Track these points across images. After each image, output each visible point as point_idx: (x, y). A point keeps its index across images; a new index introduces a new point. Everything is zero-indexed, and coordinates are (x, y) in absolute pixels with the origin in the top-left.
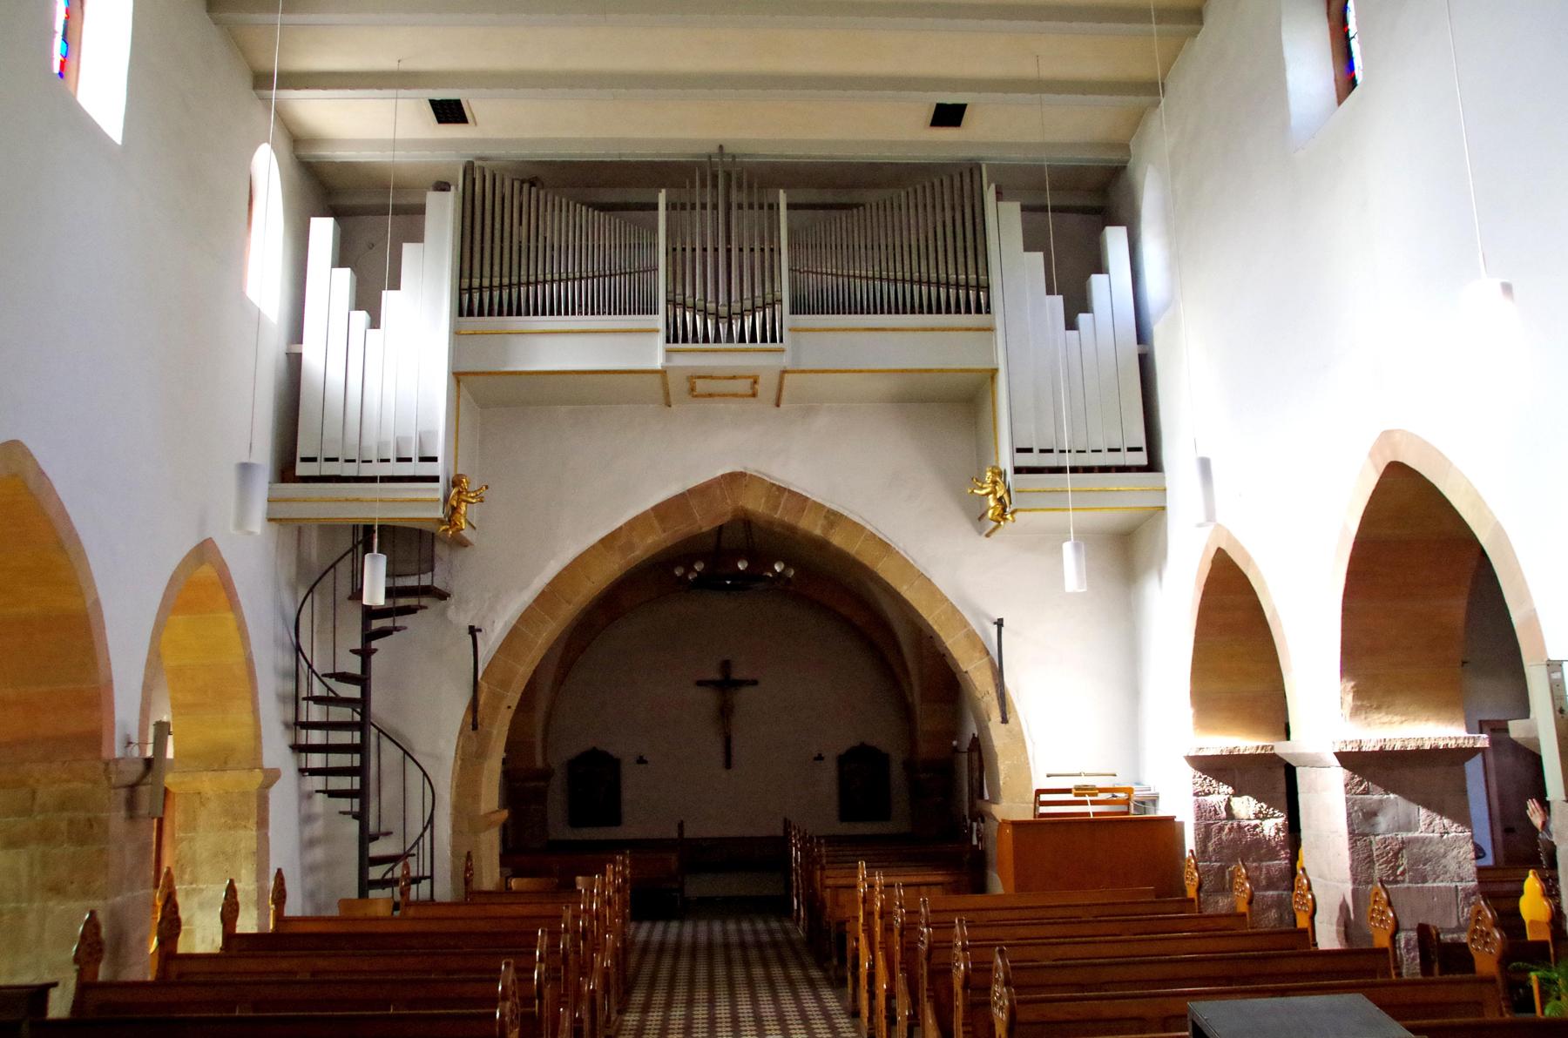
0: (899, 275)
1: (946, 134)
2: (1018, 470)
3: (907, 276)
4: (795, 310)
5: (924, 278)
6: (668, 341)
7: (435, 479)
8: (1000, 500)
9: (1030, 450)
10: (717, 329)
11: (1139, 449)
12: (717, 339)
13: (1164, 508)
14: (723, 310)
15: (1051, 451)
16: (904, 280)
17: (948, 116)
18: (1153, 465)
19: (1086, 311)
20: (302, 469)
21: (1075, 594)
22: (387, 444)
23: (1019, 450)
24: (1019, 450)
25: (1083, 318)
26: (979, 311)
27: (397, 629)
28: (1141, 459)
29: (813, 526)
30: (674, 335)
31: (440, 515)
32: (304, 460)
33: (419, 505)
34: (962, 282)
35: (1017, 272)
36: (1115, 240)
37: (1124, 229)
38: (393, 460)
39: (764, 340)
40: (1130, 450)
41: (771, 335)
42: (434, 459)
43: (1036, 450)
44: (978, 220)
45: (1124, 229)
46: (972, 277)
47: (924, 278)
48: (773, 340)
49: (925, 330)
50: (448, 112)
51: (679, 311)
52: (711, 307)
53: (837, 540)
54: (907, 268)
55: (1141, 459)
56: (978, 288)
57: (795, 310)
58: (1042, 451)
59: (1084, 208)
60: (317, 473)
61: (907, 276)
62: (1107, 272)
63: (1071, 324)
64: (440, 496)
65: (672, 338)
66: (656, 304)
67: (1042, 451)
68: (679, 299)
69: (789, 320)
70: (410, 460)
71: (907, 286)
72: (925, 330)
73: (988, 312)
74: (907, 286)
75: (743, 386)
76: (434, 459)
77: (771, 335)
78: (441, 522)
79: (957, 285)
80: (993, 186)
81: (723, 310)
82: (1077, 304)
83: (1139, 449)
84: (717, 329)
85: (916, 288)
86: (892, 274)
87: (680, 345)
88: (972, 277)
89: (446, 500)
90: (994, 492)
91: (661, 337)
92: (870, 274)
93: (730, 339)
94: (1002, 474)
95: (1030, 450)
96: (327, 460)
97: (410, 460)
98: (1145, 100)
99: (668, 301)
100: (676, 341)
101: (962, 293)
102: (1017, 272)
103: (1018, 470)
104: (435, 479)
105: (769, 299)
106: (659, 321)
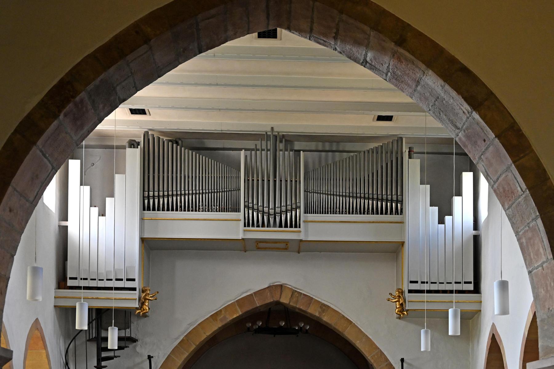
2: (410, 291)
4: (306, 212)
6: (245, 226)
7: (134, 289)
8: (401, 305)
9: (417, 282)
11: (470, 283)
13: (480, 311)
14: (272, 212)
18: (477, 290)
20: (70, 283)
22: (111, 272)
23: (411, 282)
24: (411, 282)
25: (448, 218)
32: (71, 278)
42: (134, 280)
43: (419, 282)
48: (296, 227)
49: (370, 222)
51: (250, 212)
55: (471, 287)
57: (306, 212)
63: (441, 221)
64: (137, 297)
68: (251, 205)
72: (370, 222)
76: (134, 280)
81: (272, 212)
90: (399, 301)
91: (242, 223)
94: (402, 292)
95: (417, 282)
99: (245, 206)
100: (249, 226)
103: (410, 291)
104: (134, 289)
105: (294, 206)
106: (240, 215)
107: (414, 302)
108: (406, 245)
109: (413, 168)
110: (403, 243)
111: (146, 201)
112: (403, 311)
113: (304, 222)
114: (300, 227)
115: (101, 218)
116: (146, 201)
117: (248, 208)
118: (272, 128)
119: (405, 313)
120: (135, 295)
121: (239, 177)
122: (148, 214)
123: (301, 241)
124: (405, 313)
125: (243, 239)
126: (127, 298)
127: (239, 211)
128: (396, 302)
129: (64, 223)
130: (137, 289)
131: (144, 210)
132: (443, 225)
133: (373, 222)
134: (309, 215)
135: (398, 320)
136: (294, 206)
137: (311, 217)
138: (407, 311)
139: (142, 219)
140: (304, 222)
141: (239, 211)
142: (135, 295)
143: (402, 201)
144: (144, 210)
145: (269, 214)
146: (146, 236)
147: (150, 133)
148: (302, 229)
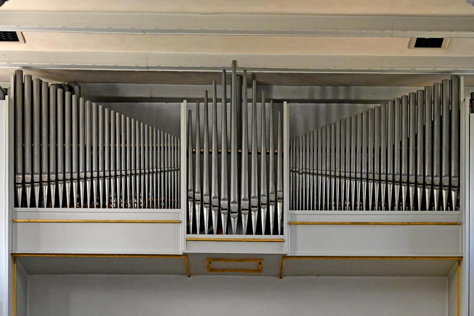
6: (188, 232)
14: (234, 207)
48: (276, 233)
49: (403, 224)
68: (198, 196)
72: (403, 224)
81: (234, 207)
91: (183, 227)
99: (188, 198)
100: (195, 232)
111: (20, 191)
114: (282, 233)
116: (20, 191)
117: (194, 201)
118: (234, 62)
122: (24, 213)
125: (185, 255)
127: (179, 207)
131: (16, 205)
133: (409, 224)
134: (297, 212)
136: (272, 197)
137: (302, 215)
139: (13, 222)
141: (179, 207)
143: (459, 186)
144: (16, 205)
146: (20, 250)
147: (25, 73)
148: (286, 236)
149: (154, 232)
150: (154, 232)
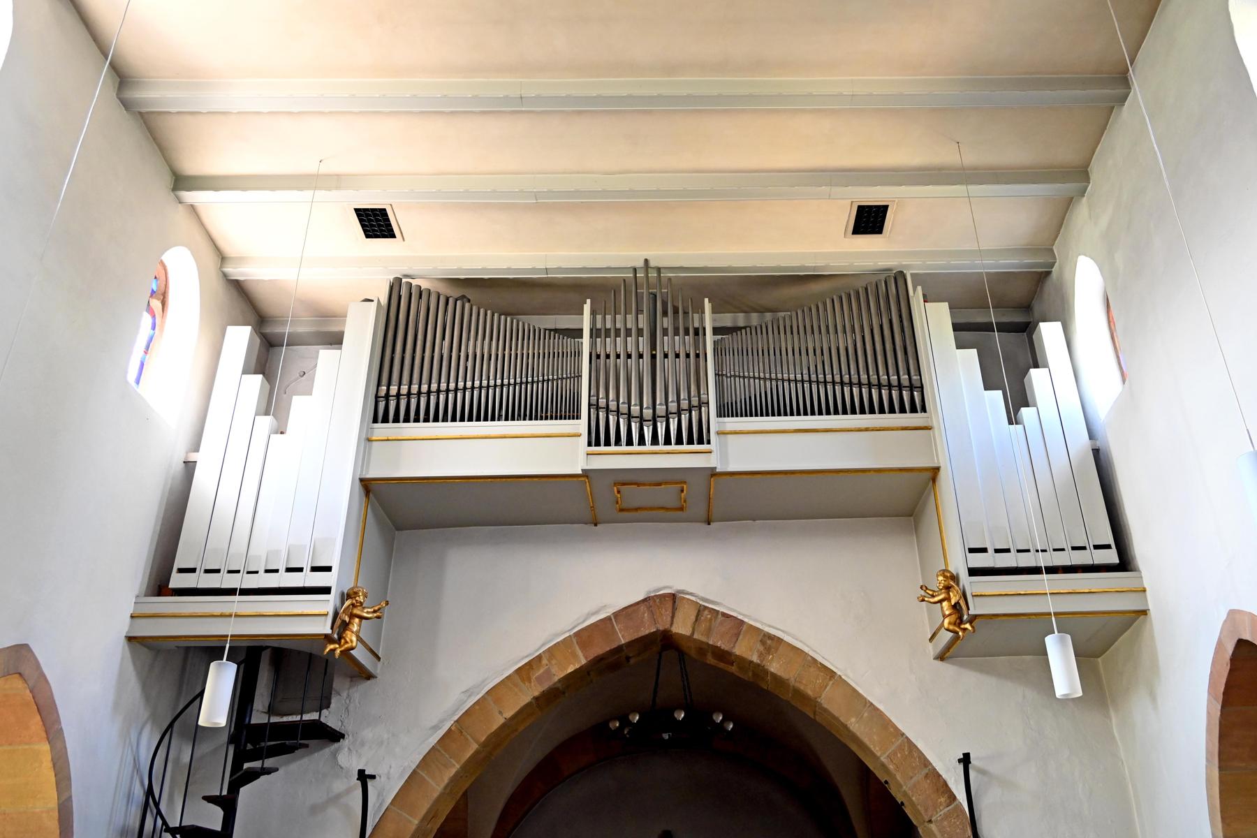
0: (829, 378)
1: (868, 243)
2: (973, 572)
3: (837, 379)
4: (719, 415)
5: (855, 380)
6: (590, 444)
7: (326, 590)
8: (956, 607)
9: (984, 550)
10: (641, 430)
11: (1108, 547)
12: (642, 441)
13: (1144, 612)
14: (648, 413)
15: (1008, 551)
16: (834, 383)
17: (870, 220)
18: (1125, 564)
19: (1027, 405)
20: (177, 581)
21: (1067, 701)
22: (277, 552)
23: (972, 550)
24: (972, 550)
26: (914, 410)
27: (268, 771)
28: (1112, 557)
29: (745, 649)
30: (595, 439)
31: (327, 630)
32: (181, 571)
33: (308, 619)
34: (895, 383)
35: (953, 371)
36: (1050, 333)
37: (1058, 325)
38: (282, 570)
39: (690, 442)
40: (1096, 547)
41: (699, 436)
42: (328, 569)
43: (991, 551)
44: (906, 323)
45: (1058, 325)
46: (904, 377)
47: (855, 380)
48: (701, 442)
49: (860, 430)
50: (376, 223)
51: (602, 415)
52: (635, 410)
53: (774, 667)
54: (836, 371)
55: (1112, 557)
56: (911, 388)
57: (719, 415)
58: (997, 551)
59: (1011, 319)
60: (193, 585)
61: (837, 379)
62: (1046, 366)
63: (1013, 419)
65: (594, 440)
66: (579, 410)
67: (997, 551)
68: (602, 402)
69: (716, 423)
70: (300, 570)
71: (838, 388)
72: (860, 430)
73: (924, 409)
74: (838, 388)
75: (666, 496)
76: (328, 569)
77: (699, 436)
78: (328, 638)
79: (890, 386)
80: (919, 288)
81: (648, 413)
82: (1018, 399)
83: (1108, 547)
84: (641, 430)
85: (847, 390)
86: (821, 376)
87: (602, 449)
88: (904, 377)
89: (336, 614)
90: (948, 599)
91: (584, 439)
92: (799, 377)
93: (655, 441)
94: (955, 578)
95: (984, 550)
96: (207, 571)
97: (300, 570)
98: (1070, 187)
99: (590, 405)
100: (598, 444)
101: (895, 393)
102: (953, 371)
103: (973, 572)
104: (326, 590)
105: (695, 401)
106: (581, 425)
107: (989, 597)
108: (943, 476)
109: (934, 323)
110: (936, 470)
111: (382, 405)
112: (961, 622)
113: (718, 433)
114: (709, 442)
115: (276, 438)
116: (382, 405)
117: (598, 408)
118: (646, 260)
119: (968, 626)
120: (327, 604)
121: (578, 354)
122: (382, 430)
123: (713, 473)
124: (968, 626)
125: (586, 473)
126: (306, 612)
127: (578, 417)
128: (941, 601)
129: (193, 457)
130: (333, 591)
131: (375, 421)
132: (1020, 427)
133: (867, 430)
134: (726, 419)
135: (938, 663)
136: (695, 401)
137: (732, 423)
138: (972, 619)
139: (368, 439)
140: (718, 433)
141: (578, 417)
142: (327, 604)
143: (922, 387)
144: (375, 421)
145: (642, 420)
146: (372, 474)
147: (404, 280)
148: (711, 447)
149: (547, 449)
150: (547, 449)
